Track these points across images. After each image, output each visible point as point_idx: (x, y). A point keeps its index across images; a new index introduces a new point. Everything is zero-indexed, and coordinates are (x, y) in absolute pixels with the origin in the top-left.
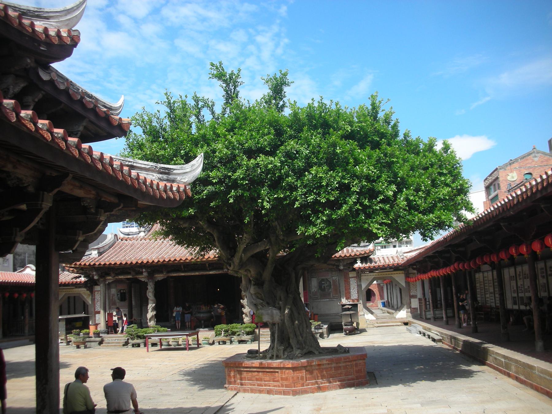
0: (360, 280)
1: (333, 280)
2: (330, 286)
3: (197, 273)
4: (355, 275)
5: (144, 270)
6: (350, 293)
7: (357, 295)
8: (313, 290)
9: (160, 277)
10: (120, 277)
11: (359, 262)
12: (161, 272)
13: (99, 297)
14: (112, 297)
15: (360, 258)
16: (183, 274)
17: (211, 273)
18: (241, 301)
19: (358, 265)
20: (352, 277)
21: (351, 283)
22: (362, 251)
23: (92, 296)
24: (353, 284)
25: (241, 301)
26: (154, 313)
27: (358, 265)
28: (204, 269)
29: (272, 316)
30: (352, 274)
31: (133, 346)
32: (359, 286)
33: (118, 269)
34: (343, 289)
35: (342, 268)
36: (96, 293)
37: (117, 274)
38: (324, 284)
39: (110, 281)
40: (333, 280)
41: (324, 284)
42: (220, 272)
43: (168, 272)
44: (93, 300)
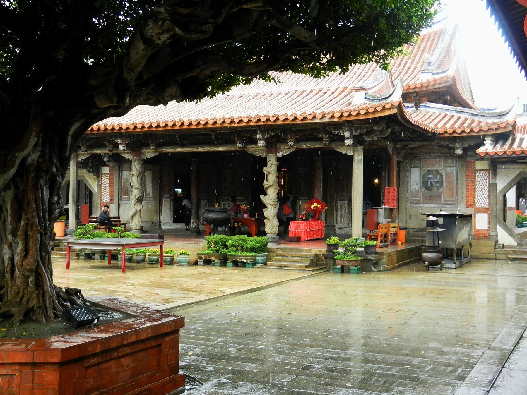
0: (495, 174)
1: (447, 174)
2: (441, 182)
3: (201, 149)
4: (487, 167)
5: (119, 141)
6: (474, 196)
7: (486, 201)
8: (413, 188)
11: (488, 142)
13: (106, 181)
14: (124, 183)
15: (492, 135)
16: (180, 150)
17: (221, 149)
18: (262, 197)
19: (488, 147)
20: (481, 170)
21: (478, 179)
22: (495, 123)
23: (99, 181)
24: (482, 182)
25: (262, 197)
27: (488, 147)
30: (480, 165)
32: (493, 187)
33: (90, 139)
34: (462, 188)
35: (459, 152)
36: (104, 176)
38: (432, 178)
40: (447, 174)
41: (432, 178)
43: (158, 146)
44: (100, 186)
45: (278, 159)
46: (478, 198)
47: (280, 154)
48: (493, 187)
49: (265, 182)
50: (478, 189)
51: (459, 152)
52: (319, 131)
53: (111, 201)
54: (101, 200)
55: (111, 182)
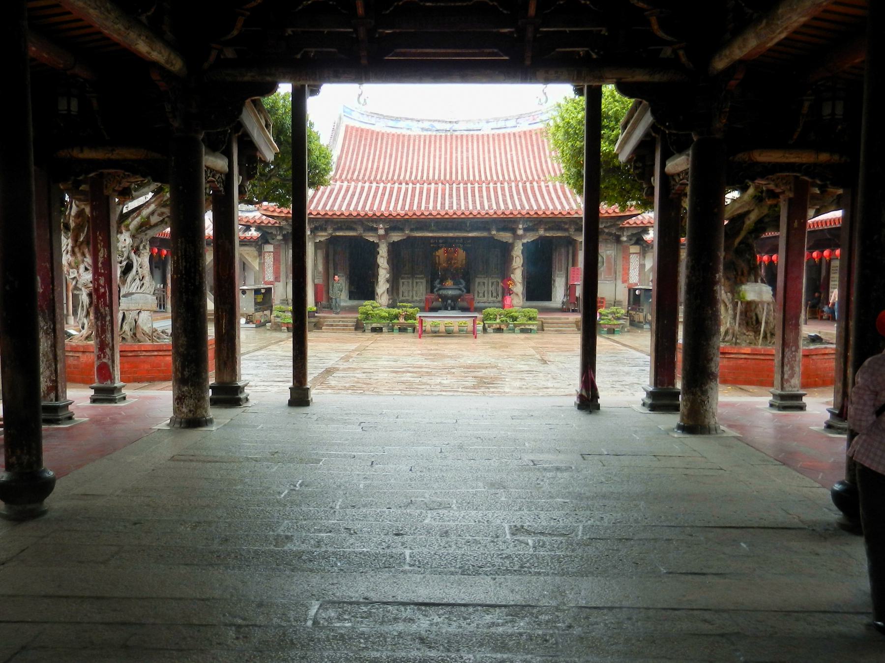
1: (608, 256)
5: (381, 226)
6: (628, 274)
7: (637, 278)
9: (396, 237)
10: (338, 234)
12: (402, 230)
13: (269, 260)
16: (430, 235)
21: (631, 261)
23: (261, 259)
26: (388, 286)
28: (447, 229)
29: (760, 293)
31: (374, 330)
32: (642, 266)
33: (337, 222)
34: (620, 268)
36: (267, 254)
37: (335, 230)
39: (322, 239)
40: (608, 256)
42: (485, 234)
44: (262, 265)
45: (523, 244)
46: (631, 275)
47: (525, 241)
48: (642, 266)
49: (514, 264)
50: (631, 268)
51: (624, 239)
52: (565, 223)
53: (277, 279)
54: (264, 278)
55: (276, 261)
